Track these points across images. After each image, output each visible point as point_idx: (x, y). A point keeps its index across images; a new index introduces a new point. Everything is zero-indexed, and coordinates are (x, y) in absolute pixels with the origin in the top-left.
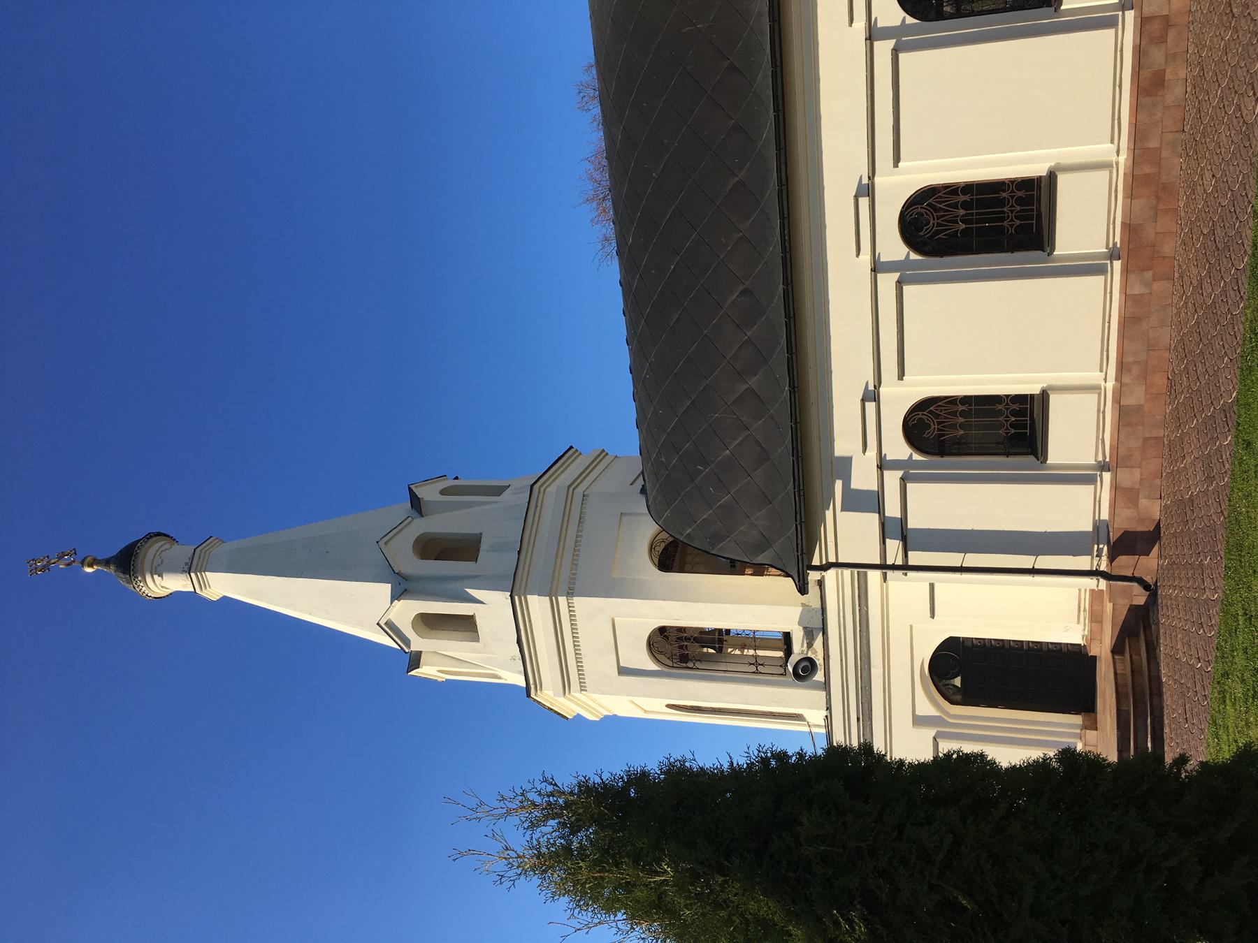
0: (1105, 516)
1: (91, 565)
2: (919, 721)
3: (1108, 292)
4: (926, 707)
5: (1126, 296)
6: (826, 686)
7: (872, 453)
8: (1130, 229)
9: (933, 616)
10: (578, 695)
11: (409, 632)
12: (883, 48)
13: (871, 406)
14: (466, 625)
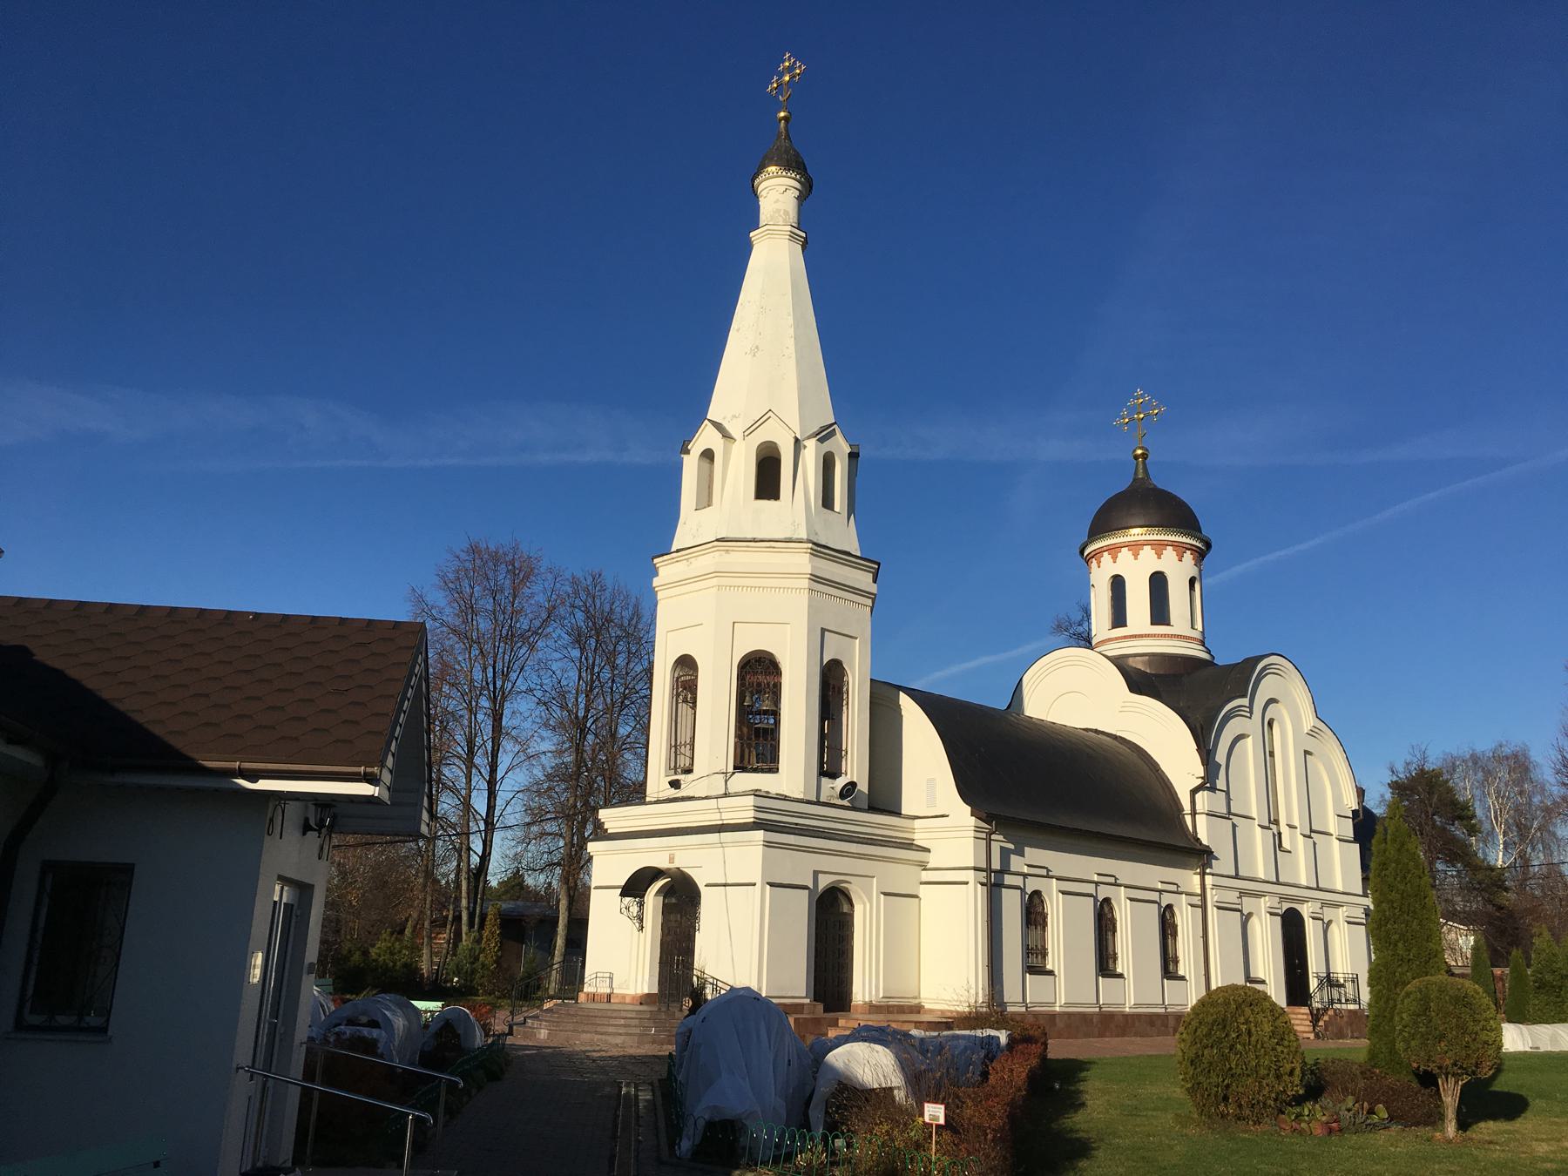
0: (1010, 1009)
1: (785, 118)
2: (816, 873)
3: (1090, 1005)
4: (824, 882)
5: (1092, 1014)
6: (818, 803)
7: (1026, 870)
8: (1111, 1016)
9: (885, 894)
10: (805, 583)
11: (828, 446)
12: (1154, 896)
13: (1044, 872)
14: (827, 502)
